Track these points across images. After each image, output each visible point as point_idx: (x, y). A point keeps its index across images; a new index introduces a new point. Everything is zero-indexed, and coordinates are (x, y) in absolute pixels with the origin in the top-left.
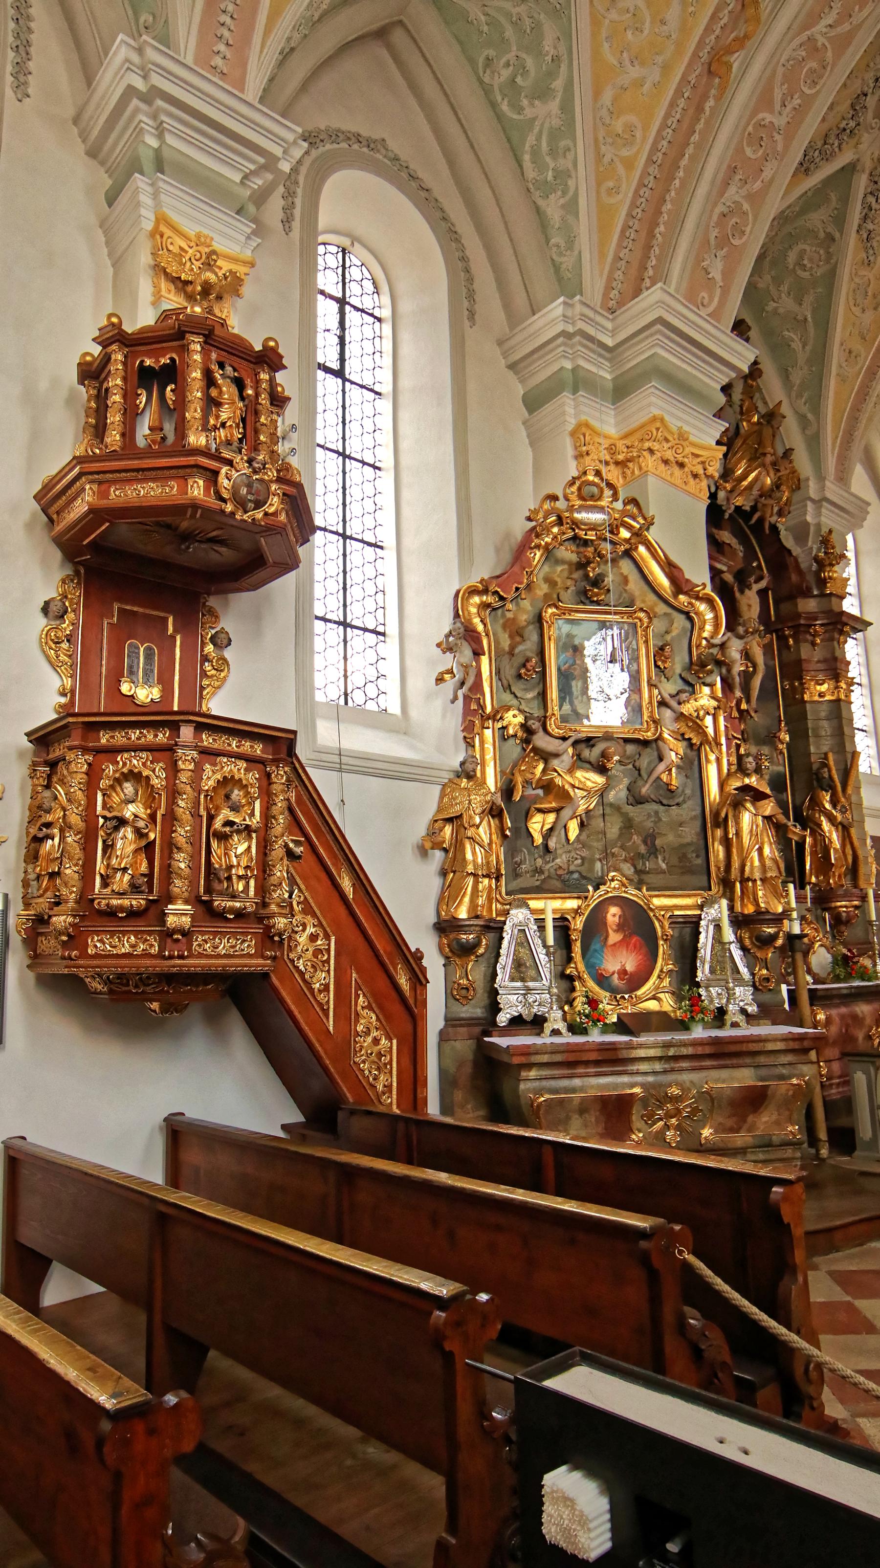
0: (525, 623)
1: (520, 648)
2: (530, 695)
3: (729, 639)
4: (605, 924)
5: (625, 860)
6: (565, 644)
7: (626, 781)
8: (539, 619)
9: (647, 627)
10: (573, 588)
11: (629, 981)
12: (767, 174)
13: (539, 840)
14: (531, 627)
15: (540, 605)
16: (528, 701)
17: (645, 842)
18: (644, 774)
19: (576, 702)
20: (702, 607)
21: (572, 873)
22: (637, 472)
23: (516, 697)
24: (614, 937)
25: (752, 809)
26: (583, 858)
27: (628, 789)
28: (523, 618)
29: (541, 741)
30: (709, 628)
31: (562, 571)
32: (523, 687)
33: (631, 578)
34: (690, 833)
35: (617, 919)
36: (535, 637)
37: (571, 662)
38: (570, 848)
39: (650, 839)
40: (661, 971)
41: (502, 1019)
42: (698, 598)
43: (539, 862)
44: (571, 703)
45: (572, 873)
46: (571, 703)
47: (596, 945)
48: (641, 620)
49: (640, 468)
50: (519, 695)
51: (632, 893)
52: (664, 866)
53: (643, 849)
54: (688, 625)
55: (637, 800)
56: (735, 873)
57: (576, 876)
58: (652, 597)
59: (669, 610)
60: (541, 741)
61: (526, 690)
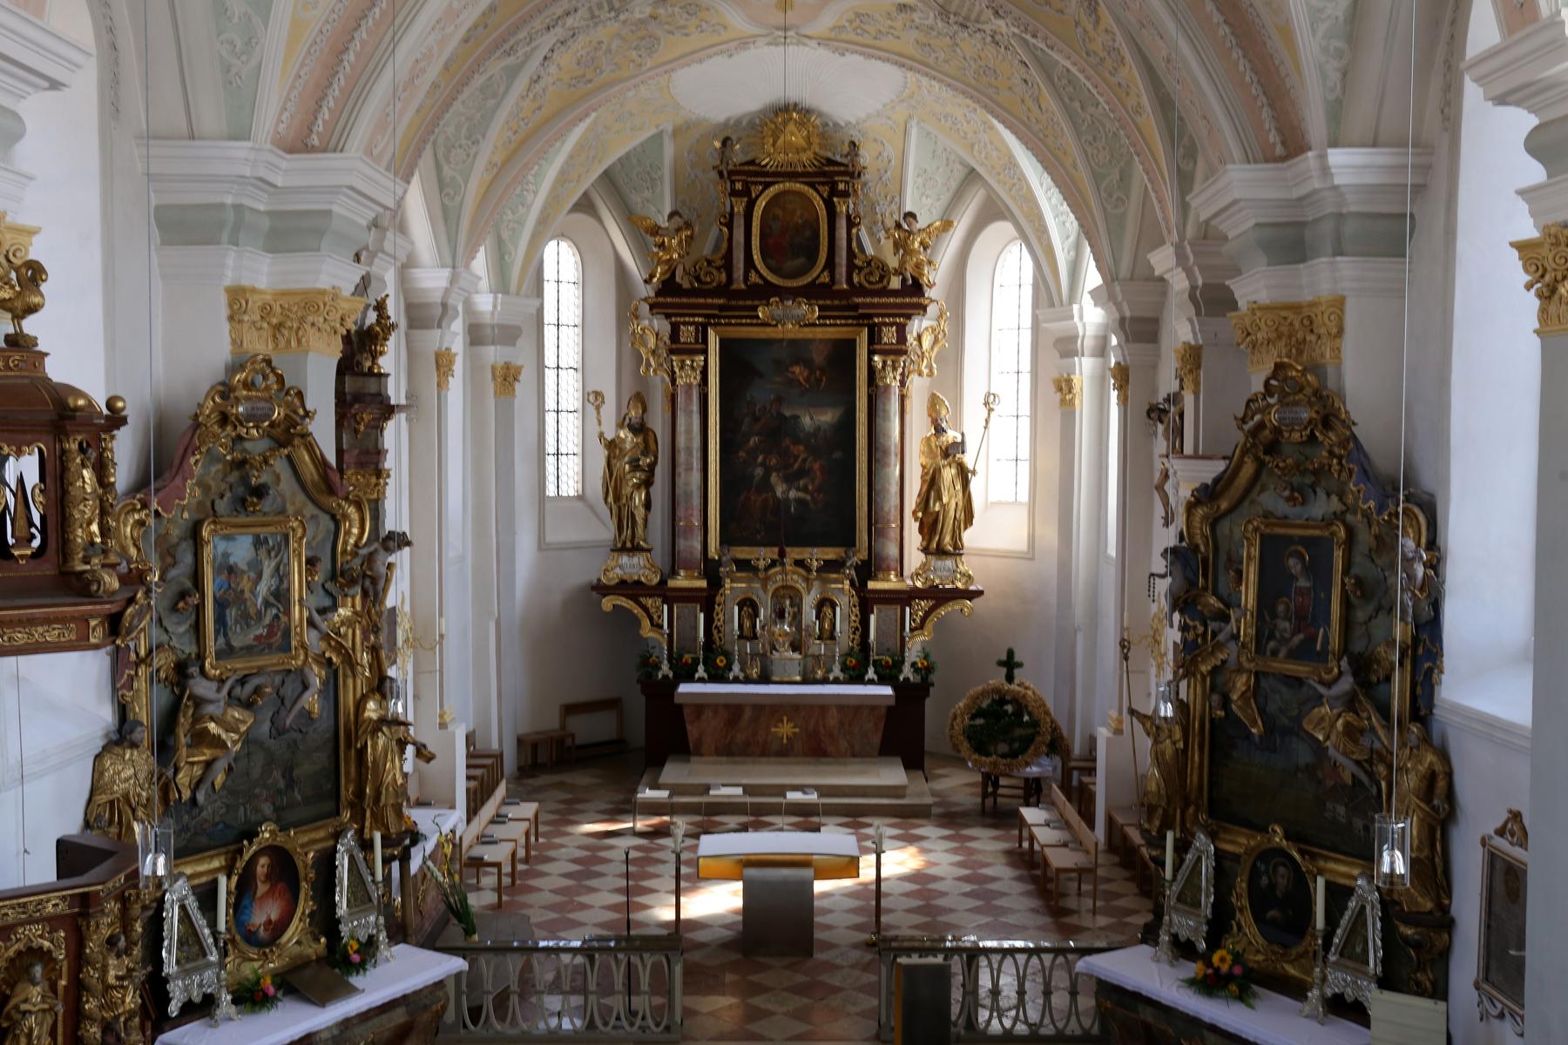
0: (175, 540)
1: (173, 573)
2: (182, 629)
3: (376, 550)
4: (255, 878)
5: (266, 800)
6: (220, 565)
7: (270, 714)
8: (194, 532)
9: (301, 538)
10: (228, 495)
11: (273, 929)
12: (461, 17)
13: (186, 794)
14: (184, 545)
15: (196, 516)
16: (180, 636)
17: (284, 777)
18: (288, 703)
19: (230, 634)
20: (352, 510)
21: (217, 824)
22: (294, 344)
23: (166, 630)
24: (262, 888)
25: (387, 733)
26: (228, 806)
27: (272, 722)
28: (175, 532)
29: (201, 687)
30: (355, 531)
31: (218, 471)
32: (175, 620)
33: (282, 477)
34: (322, 759)
35: (265, 869)
36: (188, 559)
37: (226, 586)
38: (216, 797)
39: (288, 772)
40: (303, 913)
41: (174, 1009)
42: (346, 499)
43: (186, 817)
44: (225, 635)
45: (217, 824)
46: (225, 635)
47: (246, 902)
48: (294, 530)
49: (299, 341)
50: (170, 629)
51: (280, 839)
52: (299, 798)
53: (282, 784)
54: (332, 526)
55: (278, 731)
56: (368, 801)
57: (221, 826)
58: (301, 497)
59: (316, 511)
60: (201, 687)
61: (179, 624)
